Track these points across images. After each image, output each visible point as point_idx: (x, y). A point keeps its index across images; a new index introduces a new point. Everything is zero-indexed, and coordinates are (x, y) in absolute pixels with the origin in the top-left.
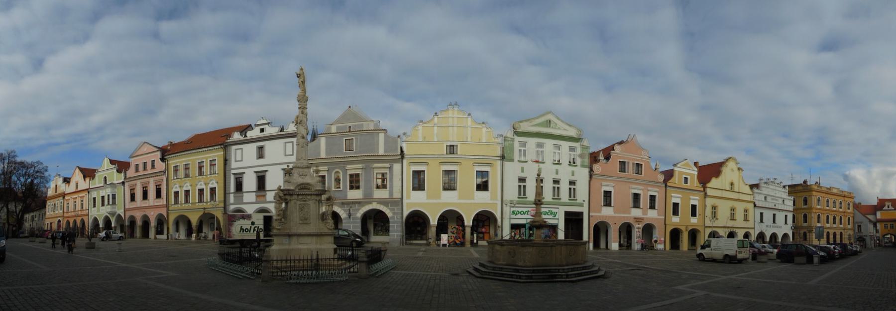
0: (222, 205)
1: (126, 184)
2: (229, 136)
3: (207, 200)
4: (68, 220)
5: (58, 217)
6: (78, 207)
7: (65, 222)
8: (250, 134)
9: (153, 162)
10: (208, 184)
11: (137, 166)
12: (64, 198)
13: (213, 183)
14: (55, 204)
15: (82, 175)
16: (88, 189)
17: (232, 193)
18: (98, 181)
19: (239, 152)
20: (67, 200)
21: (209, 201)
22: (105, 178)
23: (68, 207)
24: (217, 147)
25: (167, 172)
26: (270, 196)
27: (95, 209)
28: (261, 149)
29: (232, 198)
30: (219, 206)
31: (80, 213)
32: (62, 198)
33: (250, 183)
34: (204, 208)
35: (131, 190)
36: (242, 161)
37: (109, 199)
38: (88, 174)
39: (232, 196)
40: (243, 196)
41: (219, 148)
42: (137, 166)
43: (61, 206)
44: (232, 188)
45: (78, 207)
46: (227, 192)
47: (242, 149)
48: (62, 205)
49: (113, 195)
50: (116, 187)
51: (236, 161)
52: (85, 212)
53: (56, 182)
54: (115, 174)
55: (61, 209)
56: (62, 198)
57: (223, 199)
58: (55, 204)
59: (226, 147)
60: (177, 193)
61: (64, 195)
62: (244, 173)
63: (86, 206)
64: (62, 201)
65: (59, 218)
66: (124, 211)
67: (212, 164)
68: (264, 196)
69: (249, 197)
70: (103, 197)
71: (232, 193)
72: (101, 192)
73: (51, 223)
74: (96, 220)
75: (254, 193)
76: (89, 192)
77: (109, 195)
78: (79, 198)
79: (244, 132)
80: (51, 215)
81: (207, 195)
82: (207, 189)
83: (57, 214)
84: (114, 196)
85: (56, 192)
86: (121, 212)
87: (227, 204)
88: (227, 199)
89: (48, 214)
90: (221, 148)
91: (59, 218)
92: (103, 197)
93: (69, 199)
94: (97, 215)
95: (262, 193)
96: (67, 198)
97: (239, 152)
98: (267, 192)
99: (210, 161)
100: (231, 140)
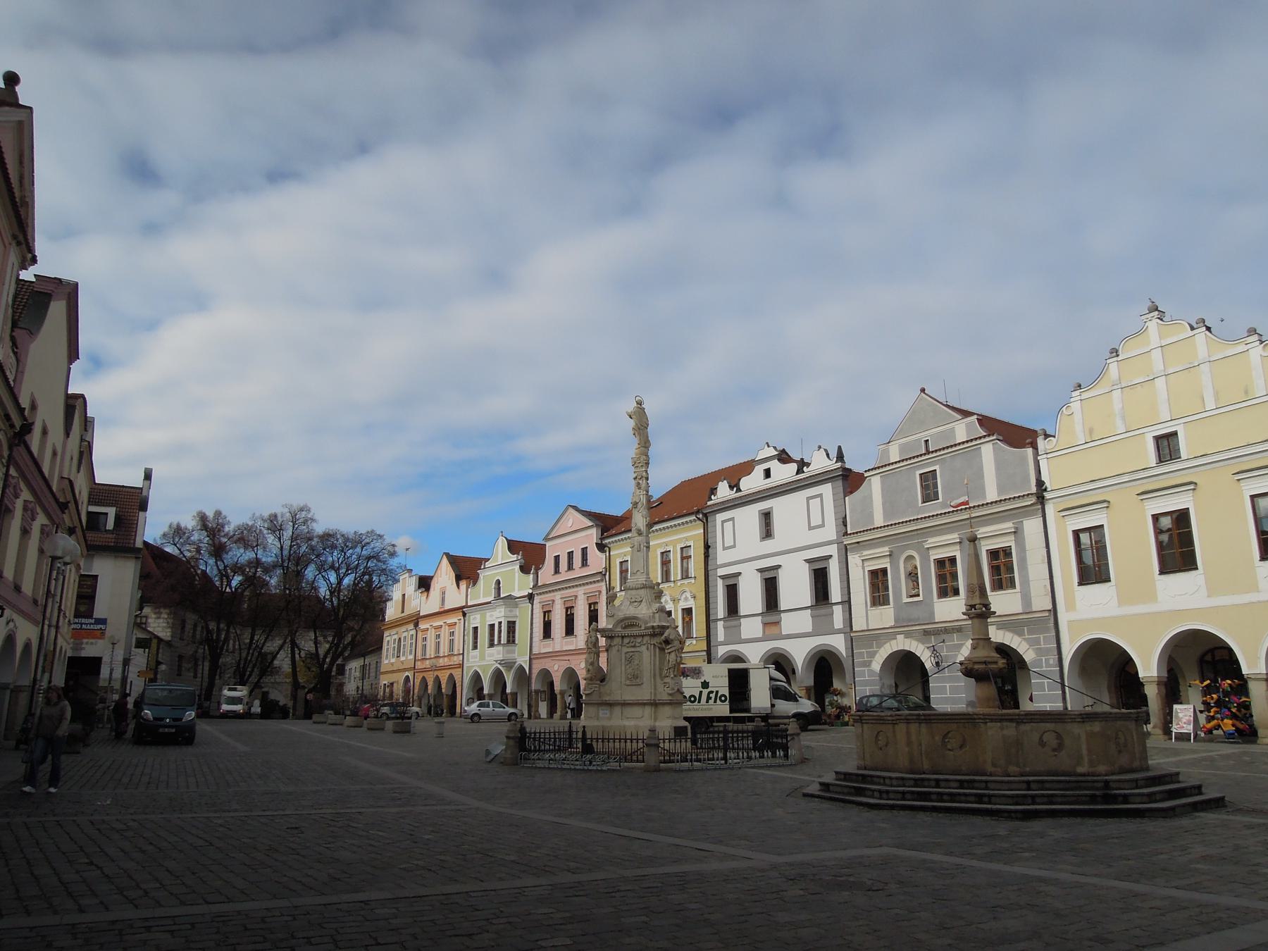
1: (537, 599)
2: (713, 491)
4: (424, 678)
5: (405, 670)
6: (444, 649)
7: (418, 682)
9: (584, 551)
11: (557, 558)
12: (416, 625)
14: (400, 639)
15: (453, 575)
16: (464, 607)
17: (720, 620)
18: (482, 591)
19: (728, 525)
20: (423, 631)
22: (498, 582)
23: (425, 647)
24: (688, 519)
25: (608, 573)
27: (476, 652)
28: (767, 516)
29: (720, 631)
31: (442, 662)
32: (411, 626)
33: (751, 597)
35: (545, 613)
36: (734, 546)
37: (500, 632)
38: (466, 570)
39: (720, 624)
42: (557, 558)
43: (411, 644)
44: (720, 609)
45: (444, 649)
46: (712, 618)
47: (732, 519)
48: (414, 641)
49: (509, 622)
50: (516, 606)
51: (725, 548)
52: (457, 660)
53: (404, 588)
54: (517, 574)
55: (411, 653)
57: (704, 633)
58: (400, 639)
59: (705, 516)
61: (416, 620)
62: (740, 574)
63: (458, 647)
64: (413, 632)
65: (407, 674)
66: (530, 659)
68: (777, 623)
69: (751, 627)
70: (492, 626)
71: (720, 620)
72: (488, 614)
74: (477, 678)
76: (464, 615)
77: (500, 623)
78: (447, 627)
80: (392, 664)
82: (676, 611)
83: (402, 662)
84: (511, 626)
85: (403, 612)
86: (523, 661)
89: (386, 662)
91: (407, 674)
92: (492, 626)
93: (427, 629)
94: (479, 666)
96: (422, 626)
97: (728, 525)
99: (682, 548)
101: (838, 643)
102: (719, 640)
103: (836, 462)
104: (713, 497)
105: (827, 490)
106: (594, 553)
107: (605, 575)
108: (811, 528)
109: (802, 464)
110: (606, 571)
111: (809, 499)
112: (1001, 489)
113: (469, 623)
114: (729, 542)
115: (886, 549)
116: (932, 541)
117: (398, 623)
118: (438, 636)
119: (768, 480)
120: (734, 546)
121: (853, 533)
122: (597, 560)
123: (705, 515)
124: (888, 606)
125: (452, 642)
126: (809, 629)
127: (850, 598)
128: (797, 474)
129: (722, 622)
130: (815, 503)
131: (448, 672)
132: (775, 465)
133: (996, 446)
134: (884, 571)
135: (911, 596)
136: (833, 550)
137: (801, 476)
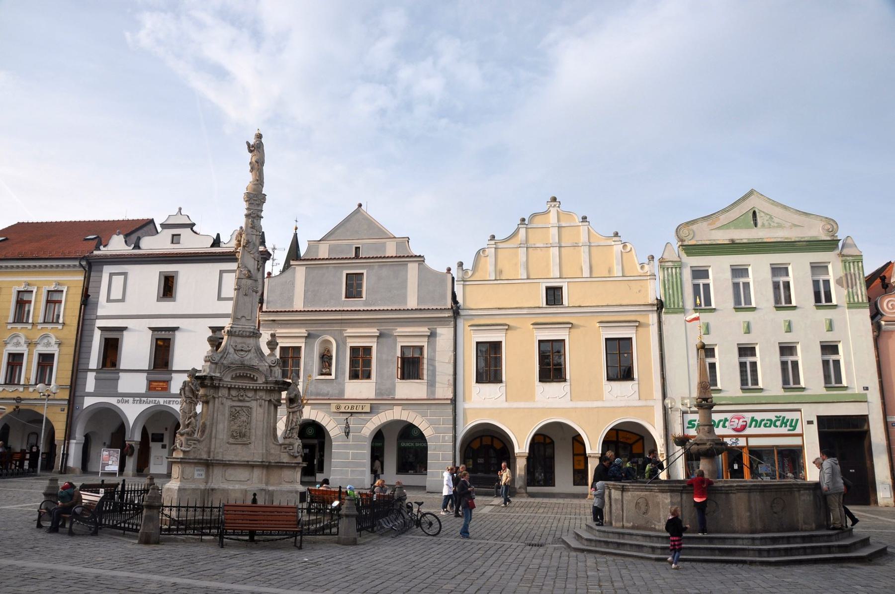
0: (66, 395)
2: (100, 242)
3: (28, 379)
8: (149, 244)
10: (36, 344)
13: (48, 344)
19: (118, 281)
21: (32, 381)
24: (71, 263)
26: (177, 383)
29: (90, 382)
30: (57, 397)
34: (19, 399)
36: (123, 300)
40: (118, 379)
41: (75, 266)
44: (94, 361)
46: (81, 367)
47: (125, 274)
51: (109, 300)
57: (68, 382)
62: (125, 328)
67: (52, 301)
75: (145, 375)
79: (134, 237)
81: (29, 370)
82: (30, 354)
87: (77, 394)
88: (79, 382)
90: (81, 265)
98: (174, 375)
100: (103, 251)
102: (86, 391)
104: (102, 248)
108: (220, 298)
112: (420, 300)
115: (304, 330)
116: (350, 331)
120: (123, 300)
123: (90, 265)
128: (212, 246)
129: (94, 374)
133: (421, 266)
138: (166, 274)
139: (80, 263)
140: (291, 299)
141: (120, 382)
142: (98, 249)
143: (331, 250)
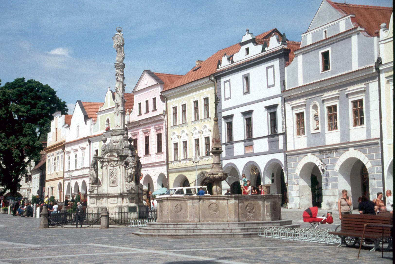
2: (219, 63)
5: (59, 179)
11: (140, 104)
12: (64, 149)
36: (230, 98)
40: (233, 148)
42: (140, 104)
47: (229, 81)
51: (226, 99)
56: (61, 150)
58: (55, 158)
60: (176, 144)
61: (62, 146)
68: (252, 146)
73: (52, 188)
75: (243, 143)
76: (90, 142)
95: (249, 143)
96: (67, 149)
97: (227, 84)
98: (255, 141)
101: (280, 157)
103: (282, 45)
104: (219, 66)
105: (276, 63)
106: (159, 101)
107: (165, 116)
108: (269, 87)
109: (266, 45)
110: (165, 113)
111: (268, 68)
113: (93, 148)
114: (227, 96)
117: (55, 148)
118: (76, 156)
119: (248, 56)
121: (288, 90)
122: (161, 106)
124: (303, 136)
125: (76, 161)
126: (266, 149)
127: (286, 131)
130: (270, 70)
131: (82, 179)
132: (251, 46)
134: (302, 113)
135: (316, 129)
136: (278, 101)
137: (264, 53)
138: (245, 76)
139: (210, 79)
140: (297, 79)
141: (235, 149)
142: (218, 68)
143: (313, 37)
